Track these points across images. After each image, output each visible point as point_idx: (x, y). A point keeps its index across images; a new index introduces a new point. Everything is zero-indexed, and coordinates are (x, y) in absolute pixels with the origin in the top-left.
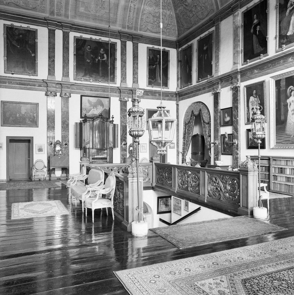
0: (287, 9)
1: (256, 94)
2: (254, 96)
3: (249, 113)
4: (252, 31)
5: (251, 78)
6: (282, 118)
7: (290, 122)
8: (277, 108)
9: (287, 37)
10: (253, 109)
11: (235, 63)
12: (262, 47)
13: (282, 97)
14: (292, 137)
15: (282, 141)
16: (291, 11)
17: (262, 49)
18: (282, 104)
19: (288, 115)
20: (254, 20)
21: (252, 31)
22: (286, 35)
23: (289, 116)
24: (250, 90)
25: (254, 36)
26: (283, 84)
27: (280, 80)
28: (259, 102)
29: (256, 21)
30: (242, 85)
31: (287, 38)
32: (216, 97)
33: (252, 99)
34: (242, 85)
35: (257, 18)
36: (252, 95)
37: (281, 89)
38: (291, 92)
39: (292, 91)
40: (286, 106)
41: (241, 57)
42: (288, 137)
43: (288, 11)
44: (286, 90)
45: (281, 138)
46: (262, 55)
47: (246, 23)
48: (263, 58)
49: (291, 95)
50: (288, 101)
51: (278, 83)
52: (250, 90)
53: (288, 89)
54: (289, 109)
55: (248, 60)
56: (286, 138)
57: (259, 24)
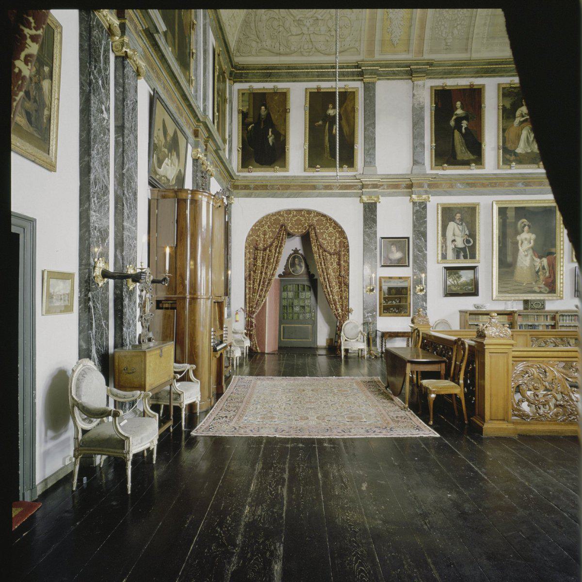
0: (514, 117)
1: (461, 220)
2: (458, 222)
3: (446, 246)
4: (452, 123)
5: (450, 194)
6: (509, 259)
7: (521, 265)
8: (501, 245)
9: (516, 154)
10: (454, 241)
11: (415, 162)
12: (473, 154)
13: (509, 231)
14: (524, 284)
15: (509, 289)
16: (521, 123)
17: (472, 157)
18: (509, 241)
19: (519, 257)
20: (457, 109)
21: (452, 123)
22: (514, 150)
23: (519, 258)
24: (448, 214)
25: (456, 133)
26: (511, 214)
27: (506, 208)
28: (467, 232)
29: (459, 112)
30: (435, 203)
31: (515, 156)
32: (370, 212)
33: (452, 225)
34: (435, 203)
35: (462, 108)
36: (453, 220)
37: (508, 221)
38: (524, 227)
39: (525, 225)
40: (516, 244)
41: (428, 156)
42: (517, 285)
43: (517, 121)
44: (516, 224)
45: (506, 286)
46: (473, 165)
47: (440, 106)
48: (474, 171)
49: (523, 231)
50: (519, 238)
51: (502, 211)
52: (448, 214)
53: (519, 223)
54: (520, 248)
55: (445, 165)
56: (515, 286)
57: (466, 118)
